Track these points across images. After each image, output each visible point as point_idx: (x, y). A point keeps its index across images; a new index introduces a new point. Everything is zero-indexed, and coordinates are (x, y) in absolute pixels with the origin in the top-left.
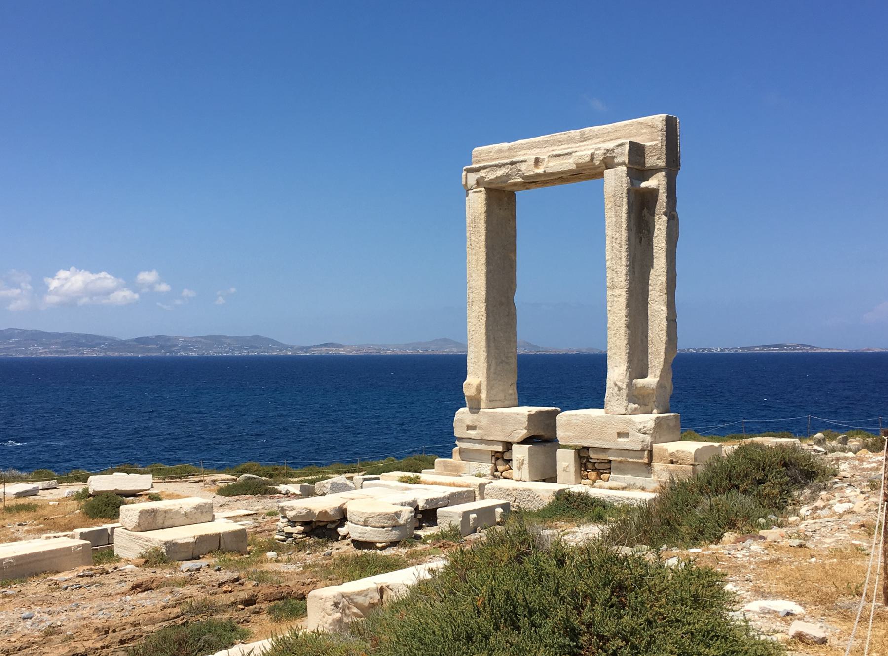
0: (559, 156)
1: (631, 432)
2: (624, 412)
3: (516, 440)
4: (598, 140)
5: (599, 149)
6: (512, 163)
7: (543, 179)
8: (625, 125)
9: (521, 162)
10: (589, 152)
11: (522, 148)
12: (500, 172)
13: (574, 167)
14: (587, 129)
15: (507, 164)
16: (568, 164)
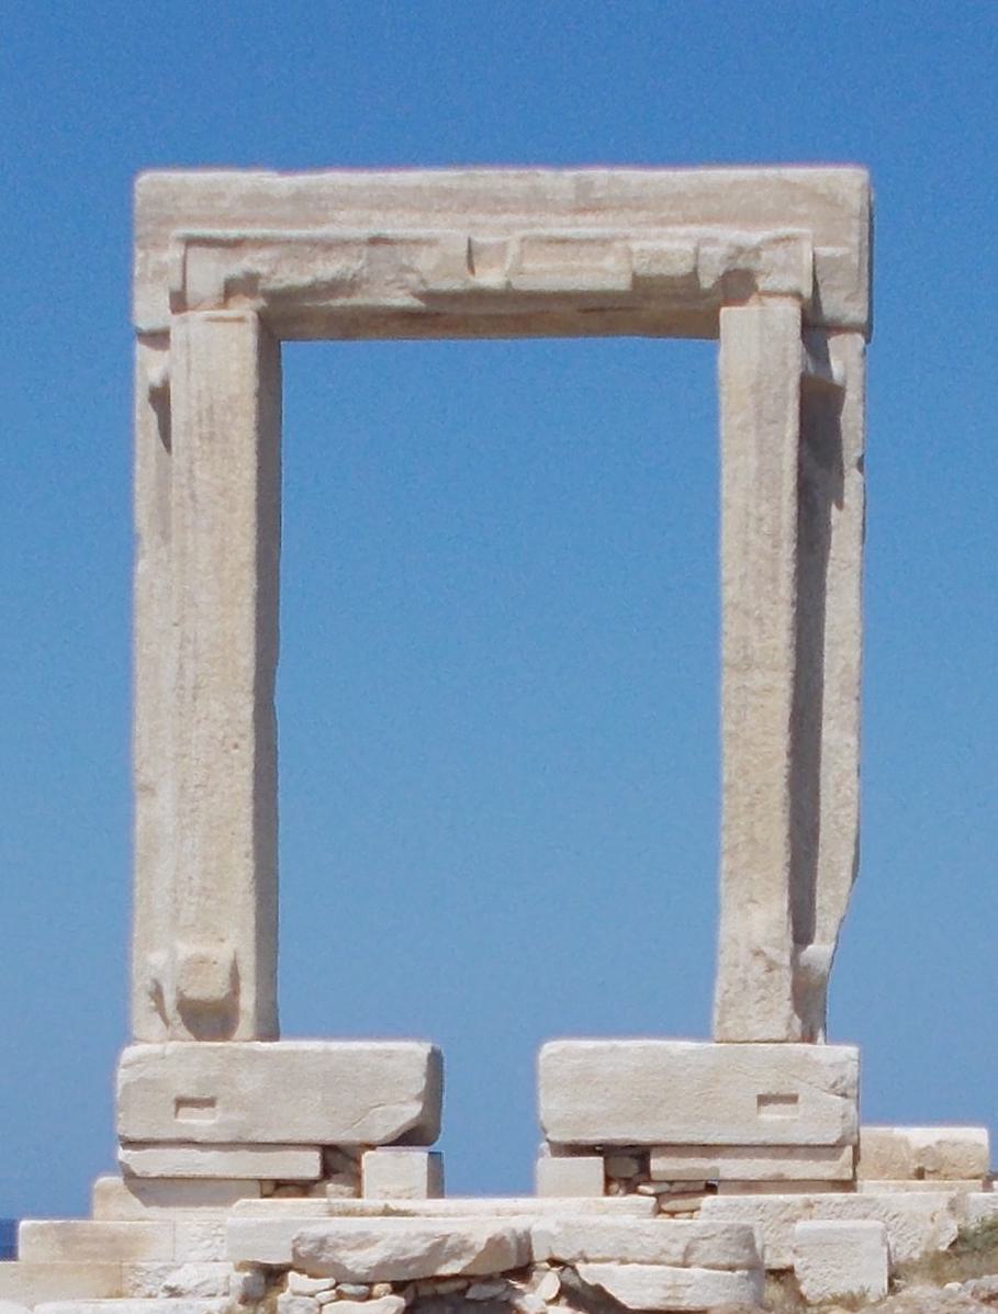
0: (564, 241)
1: (802, 1090)
2: (782, 1034)
3: (378, 1135)
4: (642, 215)
5: (713, 241)
6: (375, 241)
7: (457, 309)
8: (736, 184)
9: (417, 242)
10: (689, 247)
11: (346, 200)
12: (326, 269)
13: (622, 283)
14: (599, 175)
15: (356, 242)
16: (607, 273)
